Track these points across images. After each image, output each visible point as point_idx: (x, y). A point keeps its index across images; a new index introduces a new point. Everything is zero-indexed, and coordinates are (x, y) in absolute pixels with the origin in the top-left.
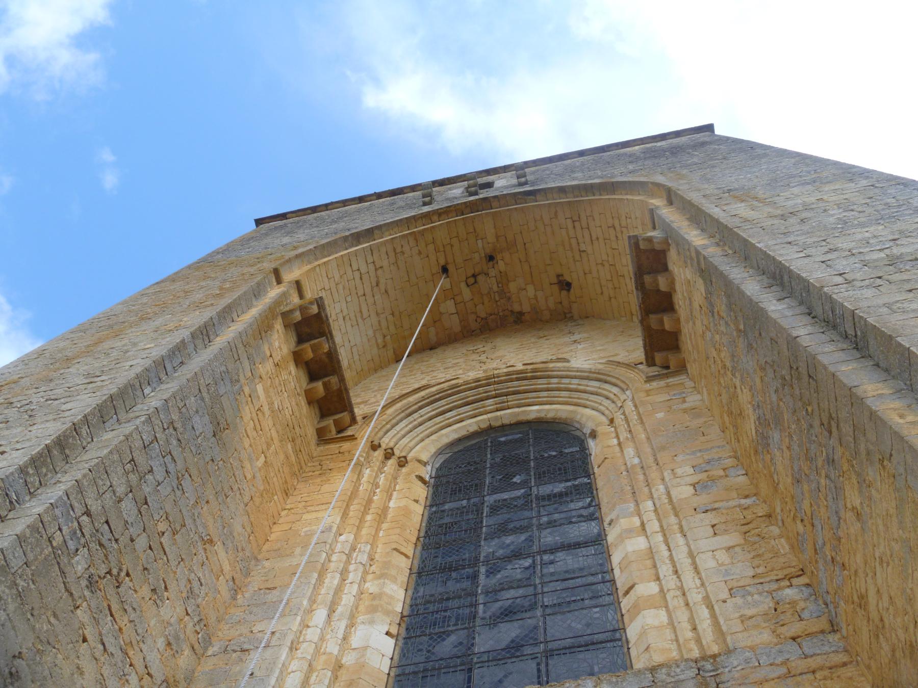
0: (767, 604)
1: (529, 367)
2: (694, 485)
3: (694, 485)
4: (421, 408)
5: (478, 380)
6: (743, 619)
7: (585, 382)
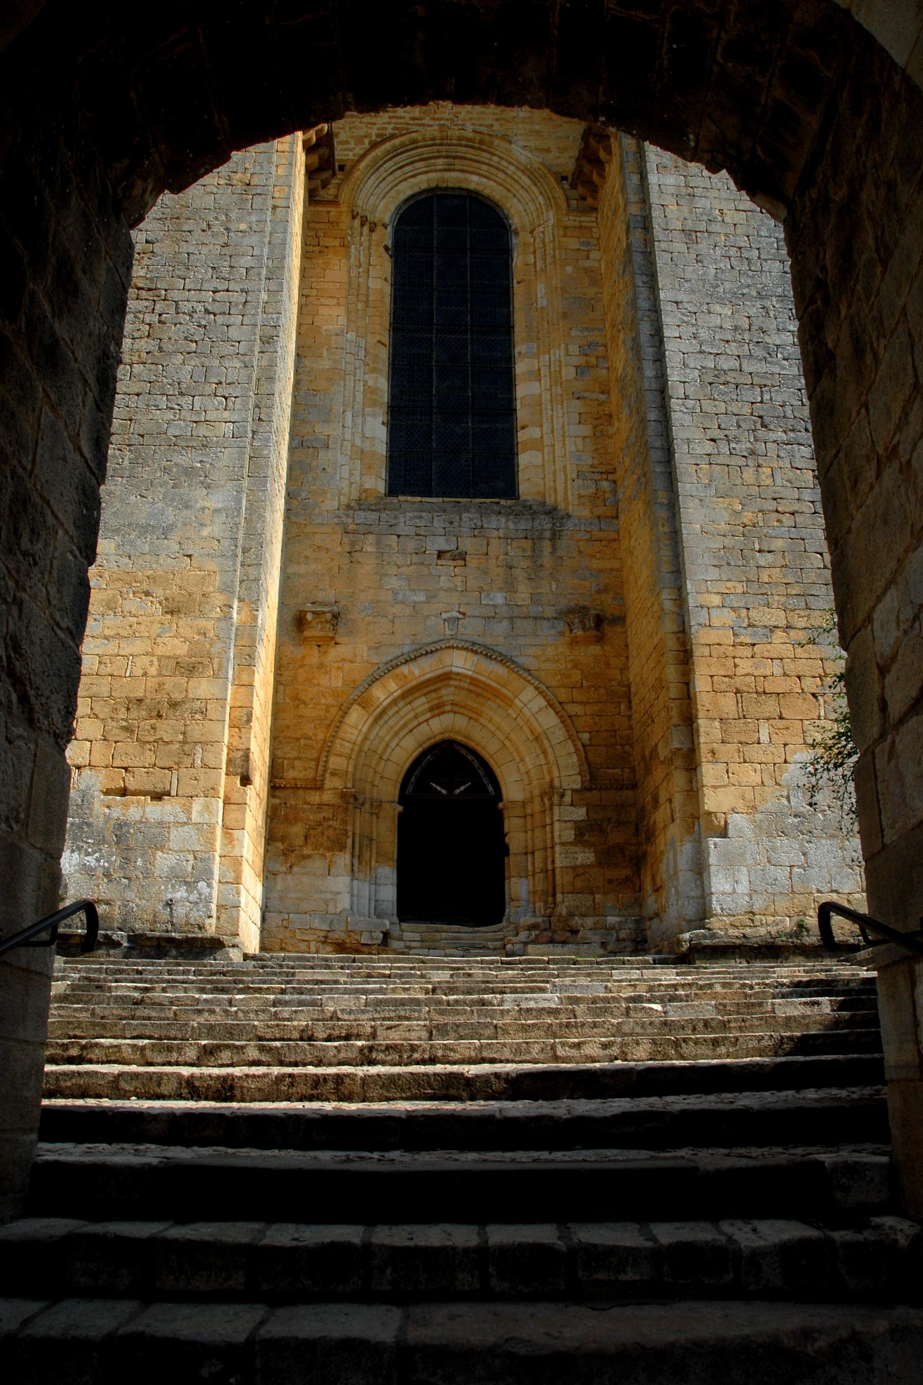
0: (592, 490)
1: (478, 137)
2: (576, 367)
3: (576, 367)
4: (385, 162)
5: (433, 139)
6: (580, 496)
7: (519, 173)
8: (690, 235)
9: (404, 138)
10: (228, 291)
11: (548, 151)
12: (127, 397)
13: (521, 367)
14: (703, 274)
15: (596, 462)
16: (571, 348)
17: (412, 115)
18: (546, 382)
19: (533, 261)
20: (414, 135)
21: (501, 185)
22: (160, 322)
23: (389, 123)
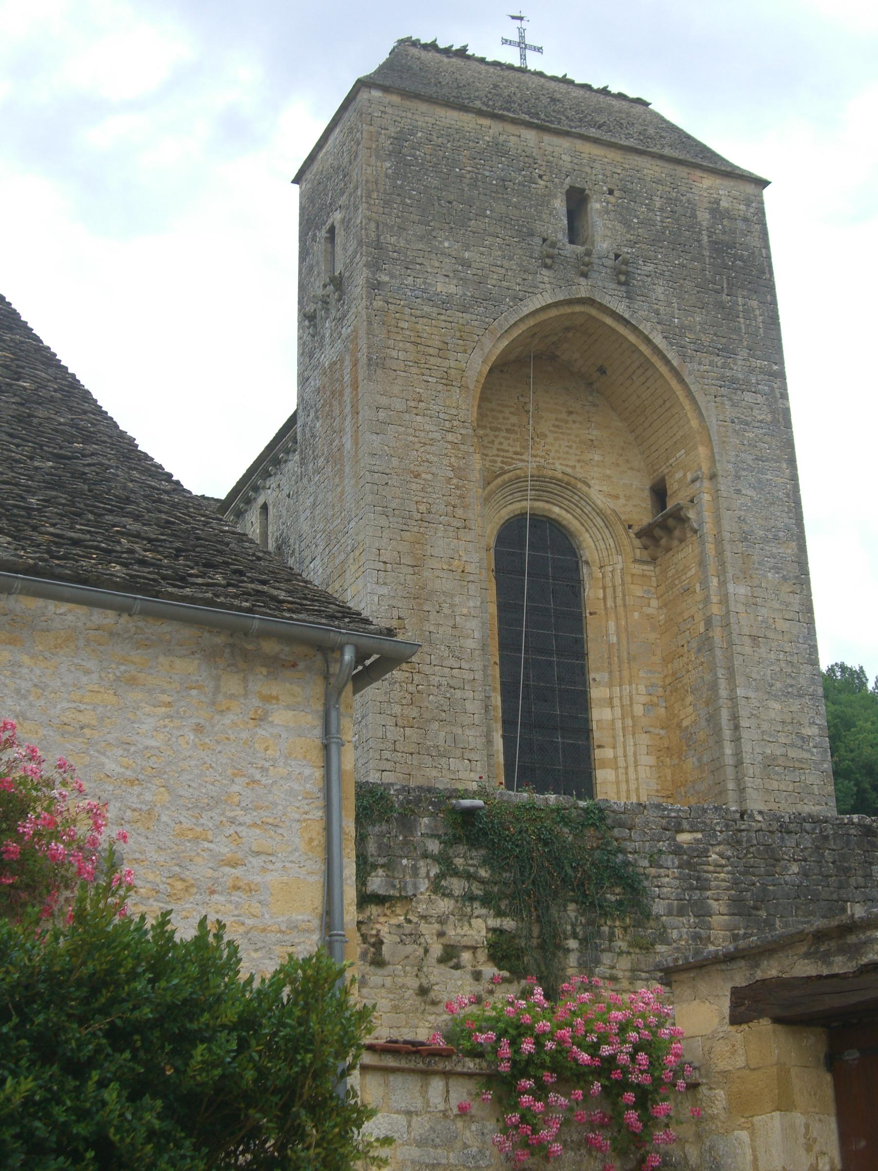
2: (644, 705)
3: (644, 705)
7: (595, 514)
8: (754, 638)
9: (511, 474)
10: (460, 668)
11: (617, 497)
12: (404, 755)
13: (596, 693)
14: (764, 675)
15: (659, 787)
16: (639, 686)
17: (514, 449)
18: (618, 711)
19: (601, 596)
20: (518, 472)
21: (577, 519)
22: (418, 692)
23: (498, 456)
